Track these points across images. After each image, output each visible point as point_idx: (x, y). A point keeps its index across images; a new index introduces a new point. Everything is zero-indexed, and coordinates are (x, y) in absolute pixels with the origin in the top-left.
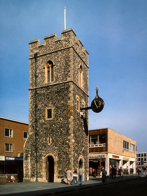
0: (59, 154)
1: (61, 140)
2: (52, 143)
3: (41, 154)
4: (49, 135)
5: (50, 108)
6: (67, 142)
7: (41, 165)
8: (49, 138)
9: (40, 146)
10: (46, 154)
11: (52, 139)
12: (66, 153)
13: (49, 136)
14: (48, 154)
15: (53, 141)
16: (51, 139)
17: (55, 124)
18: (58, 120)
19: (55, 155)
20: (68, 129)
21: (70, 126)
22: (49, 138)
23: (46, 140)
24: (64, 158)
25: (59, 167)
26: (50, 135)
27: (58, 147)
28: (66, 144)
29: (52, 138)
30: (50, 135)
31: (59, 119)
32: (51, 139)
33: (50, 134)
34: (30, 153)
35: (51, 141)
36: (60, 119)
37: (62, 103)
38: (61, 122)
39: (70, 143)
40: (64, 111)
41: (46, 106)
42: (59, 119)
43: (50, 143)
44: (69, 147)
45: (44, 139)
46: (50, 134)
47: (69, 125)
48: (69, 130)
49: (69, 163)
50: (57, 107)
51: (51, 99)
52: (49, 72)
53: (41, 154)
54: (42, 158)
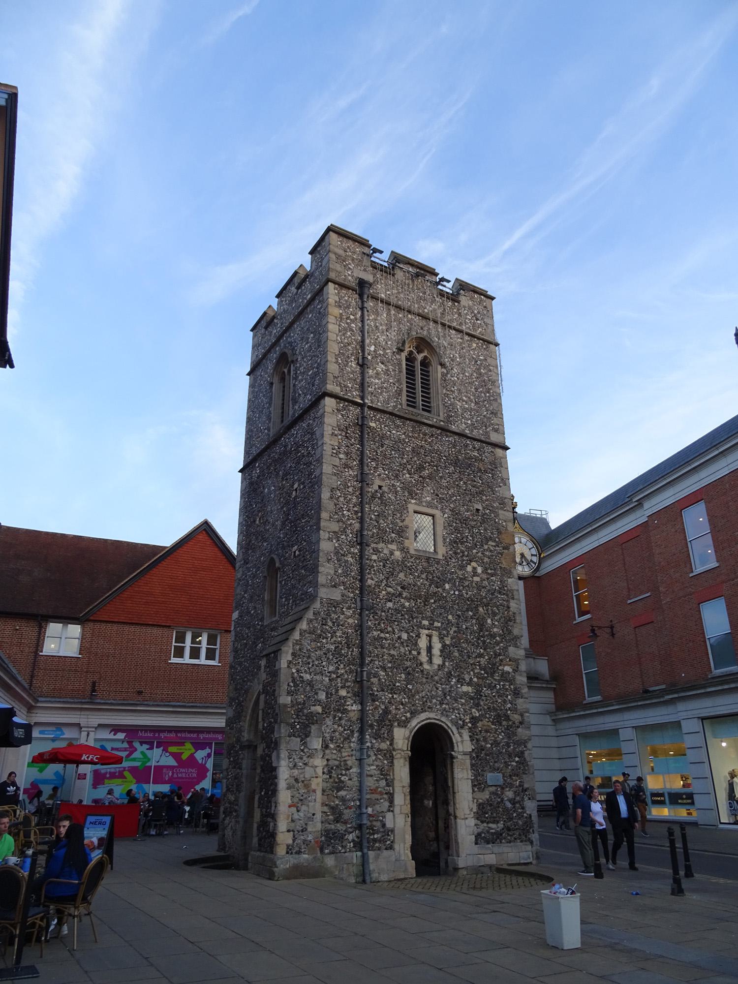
1: (481, 655)
2: (444, 663)
3: (386, 712)
4: (425, 622)
7: (386, 774)
8: (430, 636)
9: (384, 668)
10: (414, 714)
11: (444, 646)
12: (508, 718)
13: (424, 627)
14: (423, 716)
15: (445, 652)
18: (462, 567)
20: (509, 621)
22: (430, 636)
23: (413, 643)
25: (478, 784)
27: (469, 684)
29: (441, 639)
31: (469, 568)
32: (437, 646)
33: (432, 621)
35: (436, 651)
36: (474, 568)
38: (476, 579)
41: (412, 495)
42: (469, 568)
46: (432, 621)
53: (386, 712)
54: (390, 732)
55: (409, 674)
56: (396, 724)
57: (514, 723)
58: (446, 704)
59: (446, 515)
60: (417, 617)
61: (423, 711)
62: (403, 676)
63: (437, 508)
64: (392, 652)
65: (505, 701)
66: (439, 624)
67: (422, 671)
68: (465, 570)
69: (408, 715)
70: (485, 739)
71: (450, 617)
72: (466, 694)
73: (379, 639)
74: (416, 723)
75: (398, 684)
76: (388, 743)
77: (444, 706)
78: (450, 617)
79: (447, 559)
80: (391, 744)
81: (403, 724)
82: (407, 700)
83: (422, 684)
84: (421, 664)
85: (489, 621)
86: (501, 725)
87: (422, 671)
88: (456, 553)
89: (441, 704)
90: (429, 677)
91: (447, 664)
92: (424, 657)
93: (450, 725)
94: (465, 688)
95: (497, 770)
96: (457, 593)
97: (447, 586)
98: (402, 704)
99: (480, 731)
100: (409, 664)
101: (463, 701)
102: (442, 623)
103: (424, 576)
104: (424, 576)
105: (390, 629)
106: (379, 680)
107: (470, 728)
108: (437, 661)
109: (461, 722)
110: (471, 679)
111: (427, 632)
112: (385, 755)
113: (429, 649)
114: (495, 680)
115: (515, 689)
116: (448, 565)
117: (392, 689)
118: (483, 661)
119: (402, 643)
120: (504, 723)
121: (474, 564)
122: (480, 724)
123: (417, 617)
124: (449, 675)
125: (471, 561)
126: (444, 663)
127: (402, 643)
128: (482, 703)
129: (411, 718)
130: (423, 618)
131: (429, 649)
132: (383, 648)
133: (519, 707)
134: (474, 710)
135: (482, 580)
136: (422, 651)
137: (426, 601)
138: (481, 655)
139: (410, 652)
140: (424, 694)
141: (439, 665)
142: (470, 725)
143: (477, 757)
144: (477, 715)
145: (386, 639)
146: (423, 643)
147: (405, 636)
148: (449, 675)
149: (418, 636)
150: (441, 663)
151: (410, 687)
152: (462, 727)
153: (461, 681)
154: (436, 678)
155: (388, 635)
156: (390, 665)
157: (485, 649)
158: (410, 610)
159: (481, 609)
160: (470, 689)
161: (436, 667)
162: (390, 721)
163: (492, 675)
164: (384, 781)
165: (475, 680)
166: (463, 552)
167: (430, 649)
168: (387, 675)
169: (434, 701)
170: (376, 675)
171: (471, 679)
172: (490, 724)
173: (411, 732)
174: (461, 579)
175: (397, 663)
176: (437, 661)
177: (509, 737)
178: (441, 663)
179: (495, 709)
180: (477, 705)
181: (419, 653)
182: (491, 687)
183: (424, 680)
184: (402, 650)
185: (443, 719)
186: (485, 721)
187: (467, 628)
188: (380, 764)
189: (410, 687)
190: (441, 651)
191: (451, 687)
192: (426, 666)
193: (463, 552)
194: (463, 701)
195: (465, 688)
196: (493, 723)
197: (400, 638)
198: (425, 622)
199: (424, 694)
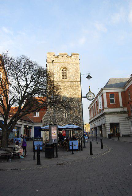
12: (79, 124)
16: (66, 115)
28: (79, 118)
29: (67, 114)
32: (66, 115)
34: (49, 123)
35: (66, 115)
43: (65, 117)
45: (61, 114)
52: (63, 73)
72: (72, 121)
73: (57, 115)
90: (65, 119)
108: (67, 117)
113: (65, 115)
118: (75, 116)
124: (69, 118)
131: (65, 115)
146: (64, 115)
147: (61, 114)
153: (71, 119)
170: (57, 120)
175: (60, 118)
176: (67, 117)
180: (73, 122)
182: (76, 119)
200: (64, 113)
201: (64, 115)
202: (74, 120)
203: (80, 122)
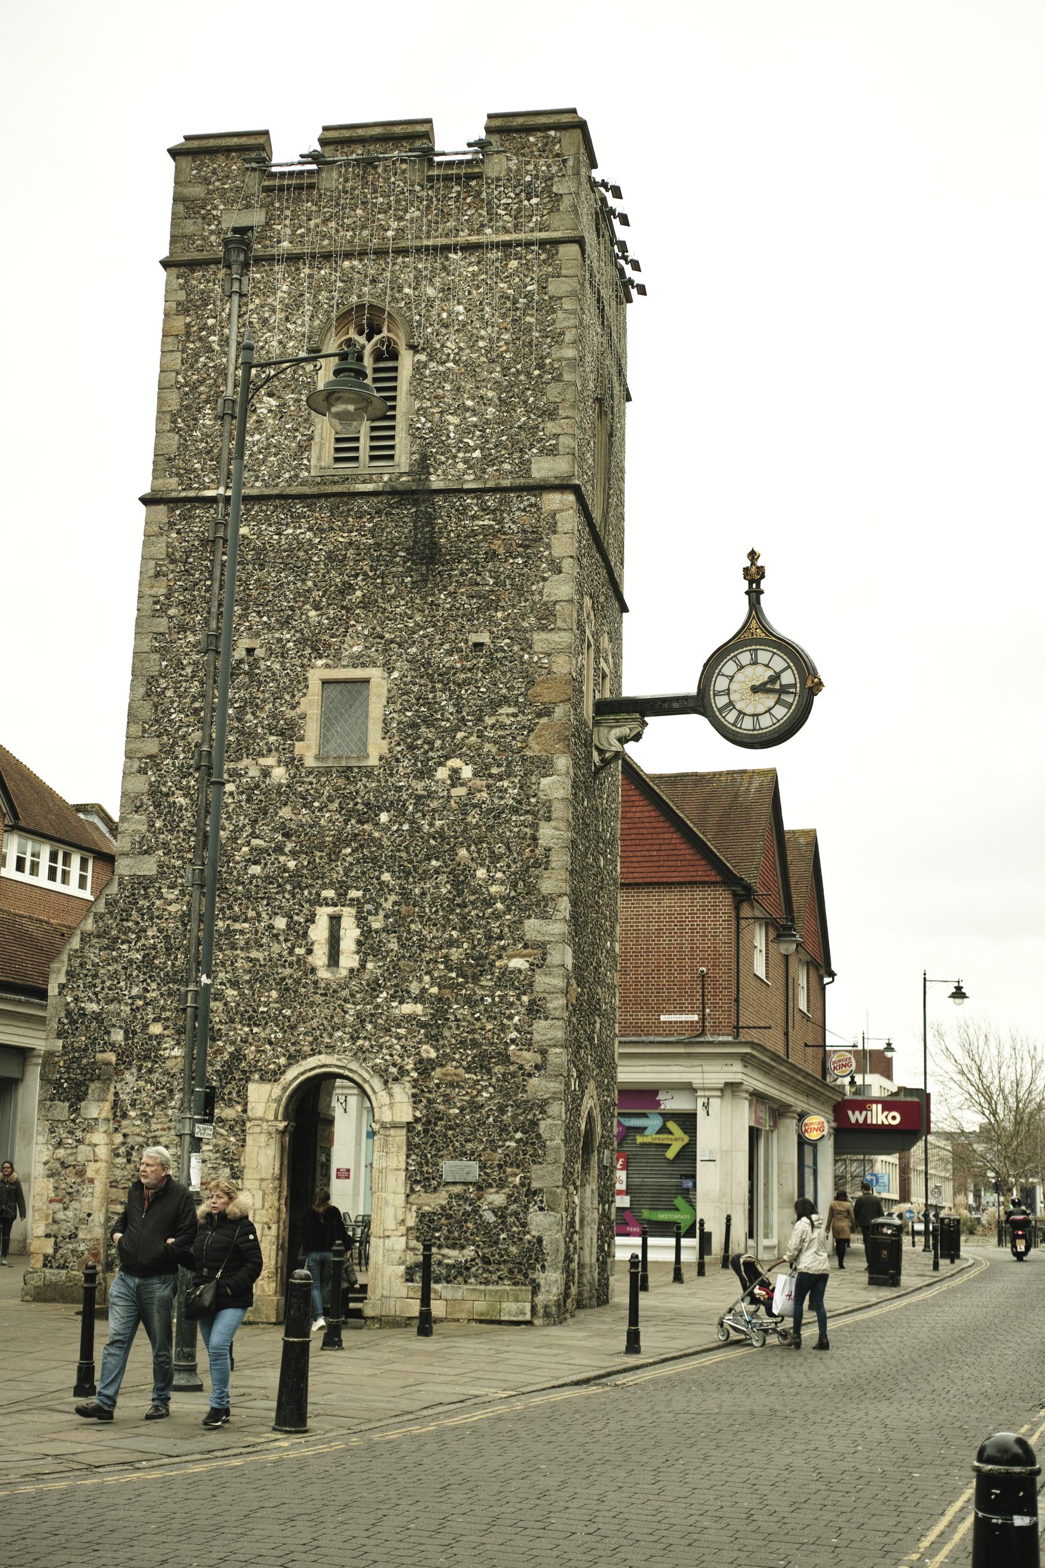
0: (425, 1067)
2: (363, 965)
3: (237, 1056)
4: (329, 893)
5: (359, 673)
6: (517, 963)
8: (335, 921)
9: (235, 984)
11: (367, 932)
12: (506, 1059)
14: (312, 1062)
15: (367, 945)
16: (350, 933)
17: (398, 809)
18: (425, 773)
19: (381, 1072)
21: (547, 833)
22: (335, 921)
23: (299, 933)
24: (474, 1106)
26: (342, 895)
27: (416, 1000)
28: (507, 978)
29: (361, 919)
30: (342, 895)
32: (350, 933)
36: (455, 771)
37: (478, 646)
38: (460, 791)
39: (542, 981)
40: (495, 705)
42: (442, 773)
44: (535, 1010)
45: (281, 923)
47: (535, 826)
48: (537, 864)
49: (533, 1145)
50: (422, 666)
51: (366, 604)
53: (237, 1056)
55: (287, 990)
56: (257, 1076)
57: (521, 1067)
58: (365, 1038)
59: (396, 674)
60: (312, 886)
61: (314, 1053)
62: (274, 994)
63: (374, 664)
64: (254, 954)
65: (503, 1028)
66: (360, 893)
67: (316, 983)
68: (431, 777)
69: (282, 1061)
70: (448, 1100)
71: (386, 877)
72: (410, 1018)
74: (294, 1075)
75: (262, 1009)
76: (239, 1108)
77: (360, 1042)
78: (386, 877)
79: (389, 763)
80: (245, 1111)
81: (272, 1076)
82: (280, 1035)
83: (312, 1004)
84: (313, 970)
85: (481, 873)
86: (489, 1071)
87: (316, 983)
88: (411, 747)
89: (354, 1039)
90: (329, 992)
91: (370, 966)
92: (320, 957)
93: (366, 1076)
94: (407, 1008)
95: (472, 1155)
96: (406, 827)
97: (384, 817)
98: (271, 1043)
99: (438, 1086)
100: (288, 971)
101: (402, 1031)
102: (366, 890)
103: (334, 806)
104: (334, 806)
105: (251, 914)
106: (225, 1004)
107: (415, 1080)
108: (349, 960)
109: (394, 1070)
110: (424, 990)
111: (330, 910)
112: (232, 1128)
114: (483, 987)
115: (532, 1002)
116: (391, 775)
117: (250, 1018)
118: (455, 954)
119: (276, 936)
120: (498, 1069)
121: (455, 763)
122: (438, 1072)
123: (312, 886)
124: (374, 987)
125: (447, 758)
126: (363, 965)
127: (276, 936)
128: (447, 1033)
129: (289, 1065)
130: (324, 886)
132: (233, 947)
133: (537, 1037)
134: (425, 1047)
135: (471, 793)
136: (315, 947)
137: (334, 855)
138: (451, 943)
139: (291, 952)
140: (314, 1023)
141: (352, 970)
142: (415, 1075)
143: (426, 1131)
144: (433, 1055)
145: (242, 932)
146: (319, 932)
148: (374, 987)
149: (311, 919)
150: (355, 964)
151: (287, 1012)
152: (396, 1079)
153: (401, 995)
154: (345, 993)
155: (246, 925)
156: (247, 978)
157: (462, 930)
158: (297, 874)
159: (463, 852)
160: (419, 1008)
161: (344, 973)
162: (244, 1072)
163: (476, 979)
164: (227, 1171)
165: (435, 990)
166: (431, 743)
167: (335, 940)
168: (242, 994)
169: (339, 1034)
171: (424, 990)
172: (461, 1071)
173: (284, 1089)
174: (419, 798)
176: (349, 960)
177: (508, 1096)
178: (355, 964)
179: (475, 1044)
180: (434, 1039)
181: (310, 952)
182: (470, 1001)
183: (318, 999)
184: (276, 948)
185: (353, 1066)
186: (450, 1068)
187: (423, 894)
188: (221, 1142)
189: (287, 1012)
190: (359, 943)
191: (378, 1006)
192: (323, 974)
193: (431, 743)
194: (402, 1031)
195: (407, 1008)
196: (468, 1069)
197: (271, 927)
198: (329, 893)
199: (314, 1023)
200: (323, 914)
201: (319, 932)
202: (440, 1008)
203: (529, 1044)
